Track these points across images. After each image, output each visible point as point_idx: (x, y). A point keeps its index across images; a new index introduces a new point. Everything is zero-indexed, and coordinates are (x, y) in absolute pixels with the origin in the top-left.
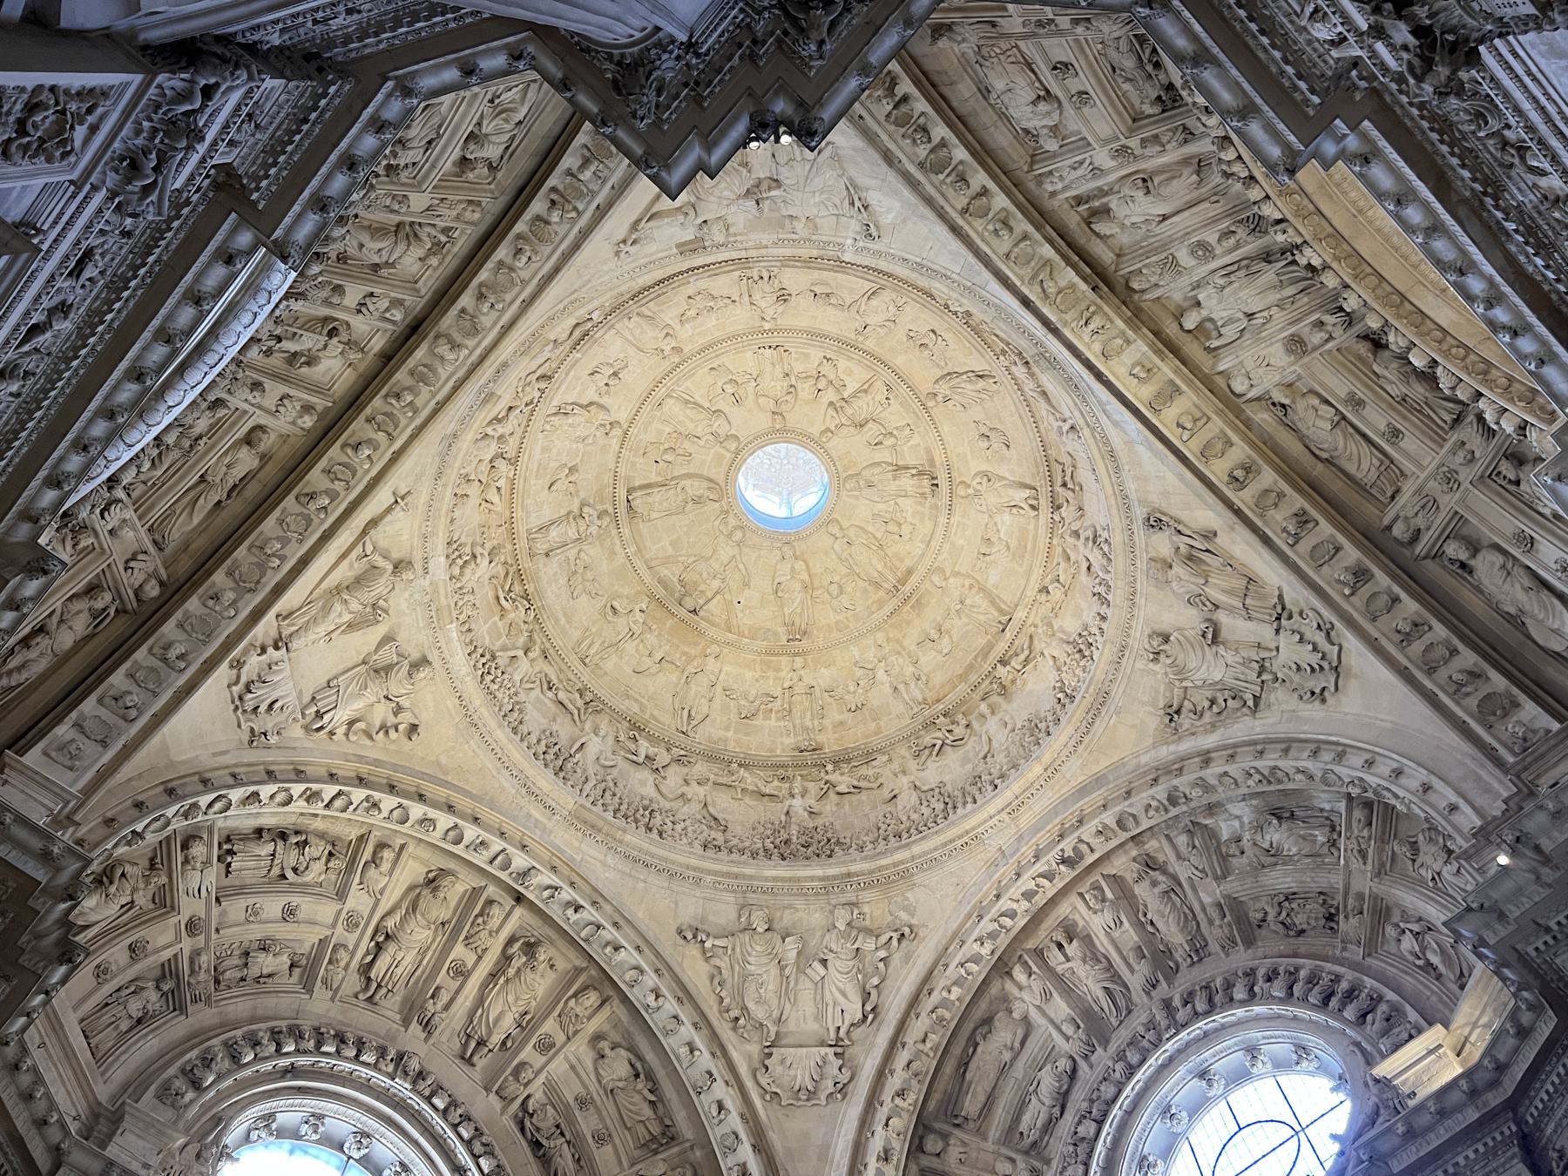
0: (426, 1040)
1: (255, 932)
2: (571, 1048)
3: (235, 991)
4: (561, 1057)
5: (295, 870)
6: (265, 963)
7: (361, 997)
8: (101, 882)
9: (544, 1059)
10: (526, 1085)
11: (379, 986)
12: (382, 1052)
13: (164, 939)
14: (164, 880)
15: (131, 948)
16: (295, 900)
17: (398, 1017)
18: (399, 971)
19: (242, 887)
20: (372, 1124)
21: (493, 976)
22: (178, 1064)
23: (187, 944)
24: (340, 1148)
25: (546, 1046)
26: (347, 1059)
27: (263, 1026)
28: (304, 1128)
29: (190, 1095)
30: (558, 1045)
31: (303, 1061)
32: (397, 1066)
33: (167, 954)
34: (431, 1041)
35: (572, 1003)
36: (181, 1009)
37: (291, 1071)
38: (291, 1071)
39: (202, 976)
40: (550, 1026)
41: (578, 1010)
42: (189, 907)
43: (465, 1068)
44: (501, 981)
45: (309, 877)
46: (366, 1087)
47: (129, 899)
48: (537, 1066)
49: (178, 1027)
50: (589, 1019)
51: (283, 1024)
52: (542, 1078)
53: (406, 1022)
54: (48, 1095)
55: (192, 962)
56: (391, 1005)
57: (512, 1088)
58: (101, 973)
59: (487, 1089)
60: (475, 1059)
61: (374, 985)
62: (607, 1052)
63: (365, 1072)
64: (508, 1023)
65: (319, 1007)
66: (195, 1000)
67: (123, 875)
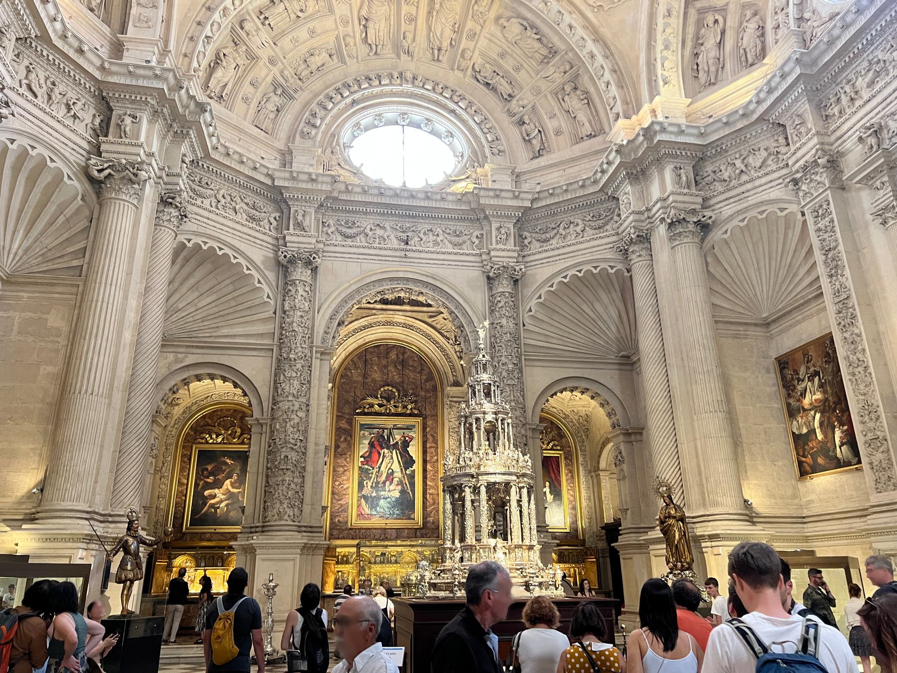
0: (412, 60)
1: (303, 49)
2: (486, 30)
3: (312, 79)
4: (482, 38)
5: (301, 11)
6: (316, 61)
7: (371, 54)
8: (218, 63)
9: (474, 43)
10: (470, 59)
11: (376, 46)
12: (391, 76)
13: (264, 73)
14: (244, 48)
15: (252, 84)
16: (311, 25)
17: (393, 55)
18: (381, 34)
19: (283, 31)
20: (405, 108)
21: (429, 13)
22: (303, 121)
23: (275, 70)
24: (397, 123)
25: (473, 36)
26: (376, 86)
27: (330, 89)
28: (376, 122)
29: (314, 132)
30: (478, 33)
31: (356, 96)
32: (401, 78)
33: (269, 79)
34: (415, 59)
35: (476, 7)
36: (291, 98)
37: (354, 102)
38: (354, 102)
39: (291, 80)
40: (470, 24)
41: (481, 9)
42: (264, 54)
43: (438, 64)
44: (435, 13)
45: (310, 11)
46: (393, 94)
47: (235, 65)
48: (472, 48)
49: (295, 106)
50: (489, 11)
51: (339, 84)
52: (477, 53)
53: (398, 56)
54: (248, 158)
55: (283, 77)
56: (387, 51)
57: (463, 64)
58: (246, 100)
59: (452, 69)
60: (440, 58)
61: (374, 47)
62: (505, 24)
63: (388, 88)
64: (448, 33)
65: (353, 68)
66: (296, 91)
67: (224, 55)
